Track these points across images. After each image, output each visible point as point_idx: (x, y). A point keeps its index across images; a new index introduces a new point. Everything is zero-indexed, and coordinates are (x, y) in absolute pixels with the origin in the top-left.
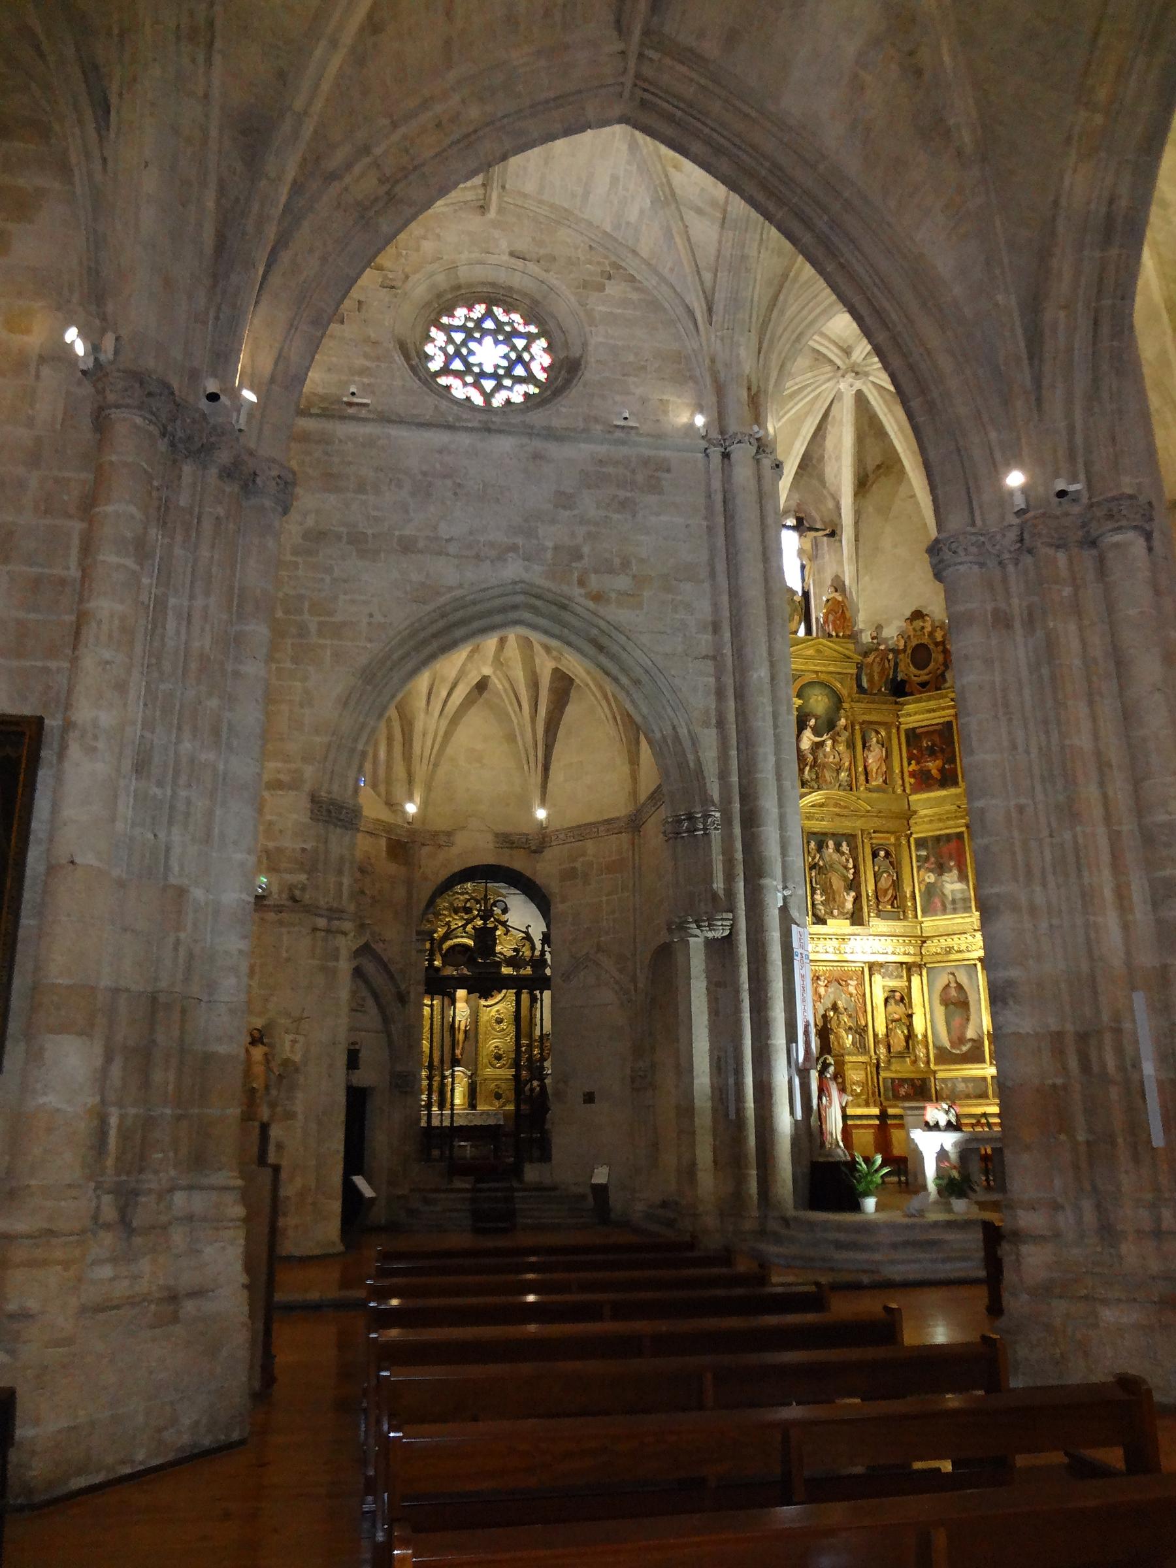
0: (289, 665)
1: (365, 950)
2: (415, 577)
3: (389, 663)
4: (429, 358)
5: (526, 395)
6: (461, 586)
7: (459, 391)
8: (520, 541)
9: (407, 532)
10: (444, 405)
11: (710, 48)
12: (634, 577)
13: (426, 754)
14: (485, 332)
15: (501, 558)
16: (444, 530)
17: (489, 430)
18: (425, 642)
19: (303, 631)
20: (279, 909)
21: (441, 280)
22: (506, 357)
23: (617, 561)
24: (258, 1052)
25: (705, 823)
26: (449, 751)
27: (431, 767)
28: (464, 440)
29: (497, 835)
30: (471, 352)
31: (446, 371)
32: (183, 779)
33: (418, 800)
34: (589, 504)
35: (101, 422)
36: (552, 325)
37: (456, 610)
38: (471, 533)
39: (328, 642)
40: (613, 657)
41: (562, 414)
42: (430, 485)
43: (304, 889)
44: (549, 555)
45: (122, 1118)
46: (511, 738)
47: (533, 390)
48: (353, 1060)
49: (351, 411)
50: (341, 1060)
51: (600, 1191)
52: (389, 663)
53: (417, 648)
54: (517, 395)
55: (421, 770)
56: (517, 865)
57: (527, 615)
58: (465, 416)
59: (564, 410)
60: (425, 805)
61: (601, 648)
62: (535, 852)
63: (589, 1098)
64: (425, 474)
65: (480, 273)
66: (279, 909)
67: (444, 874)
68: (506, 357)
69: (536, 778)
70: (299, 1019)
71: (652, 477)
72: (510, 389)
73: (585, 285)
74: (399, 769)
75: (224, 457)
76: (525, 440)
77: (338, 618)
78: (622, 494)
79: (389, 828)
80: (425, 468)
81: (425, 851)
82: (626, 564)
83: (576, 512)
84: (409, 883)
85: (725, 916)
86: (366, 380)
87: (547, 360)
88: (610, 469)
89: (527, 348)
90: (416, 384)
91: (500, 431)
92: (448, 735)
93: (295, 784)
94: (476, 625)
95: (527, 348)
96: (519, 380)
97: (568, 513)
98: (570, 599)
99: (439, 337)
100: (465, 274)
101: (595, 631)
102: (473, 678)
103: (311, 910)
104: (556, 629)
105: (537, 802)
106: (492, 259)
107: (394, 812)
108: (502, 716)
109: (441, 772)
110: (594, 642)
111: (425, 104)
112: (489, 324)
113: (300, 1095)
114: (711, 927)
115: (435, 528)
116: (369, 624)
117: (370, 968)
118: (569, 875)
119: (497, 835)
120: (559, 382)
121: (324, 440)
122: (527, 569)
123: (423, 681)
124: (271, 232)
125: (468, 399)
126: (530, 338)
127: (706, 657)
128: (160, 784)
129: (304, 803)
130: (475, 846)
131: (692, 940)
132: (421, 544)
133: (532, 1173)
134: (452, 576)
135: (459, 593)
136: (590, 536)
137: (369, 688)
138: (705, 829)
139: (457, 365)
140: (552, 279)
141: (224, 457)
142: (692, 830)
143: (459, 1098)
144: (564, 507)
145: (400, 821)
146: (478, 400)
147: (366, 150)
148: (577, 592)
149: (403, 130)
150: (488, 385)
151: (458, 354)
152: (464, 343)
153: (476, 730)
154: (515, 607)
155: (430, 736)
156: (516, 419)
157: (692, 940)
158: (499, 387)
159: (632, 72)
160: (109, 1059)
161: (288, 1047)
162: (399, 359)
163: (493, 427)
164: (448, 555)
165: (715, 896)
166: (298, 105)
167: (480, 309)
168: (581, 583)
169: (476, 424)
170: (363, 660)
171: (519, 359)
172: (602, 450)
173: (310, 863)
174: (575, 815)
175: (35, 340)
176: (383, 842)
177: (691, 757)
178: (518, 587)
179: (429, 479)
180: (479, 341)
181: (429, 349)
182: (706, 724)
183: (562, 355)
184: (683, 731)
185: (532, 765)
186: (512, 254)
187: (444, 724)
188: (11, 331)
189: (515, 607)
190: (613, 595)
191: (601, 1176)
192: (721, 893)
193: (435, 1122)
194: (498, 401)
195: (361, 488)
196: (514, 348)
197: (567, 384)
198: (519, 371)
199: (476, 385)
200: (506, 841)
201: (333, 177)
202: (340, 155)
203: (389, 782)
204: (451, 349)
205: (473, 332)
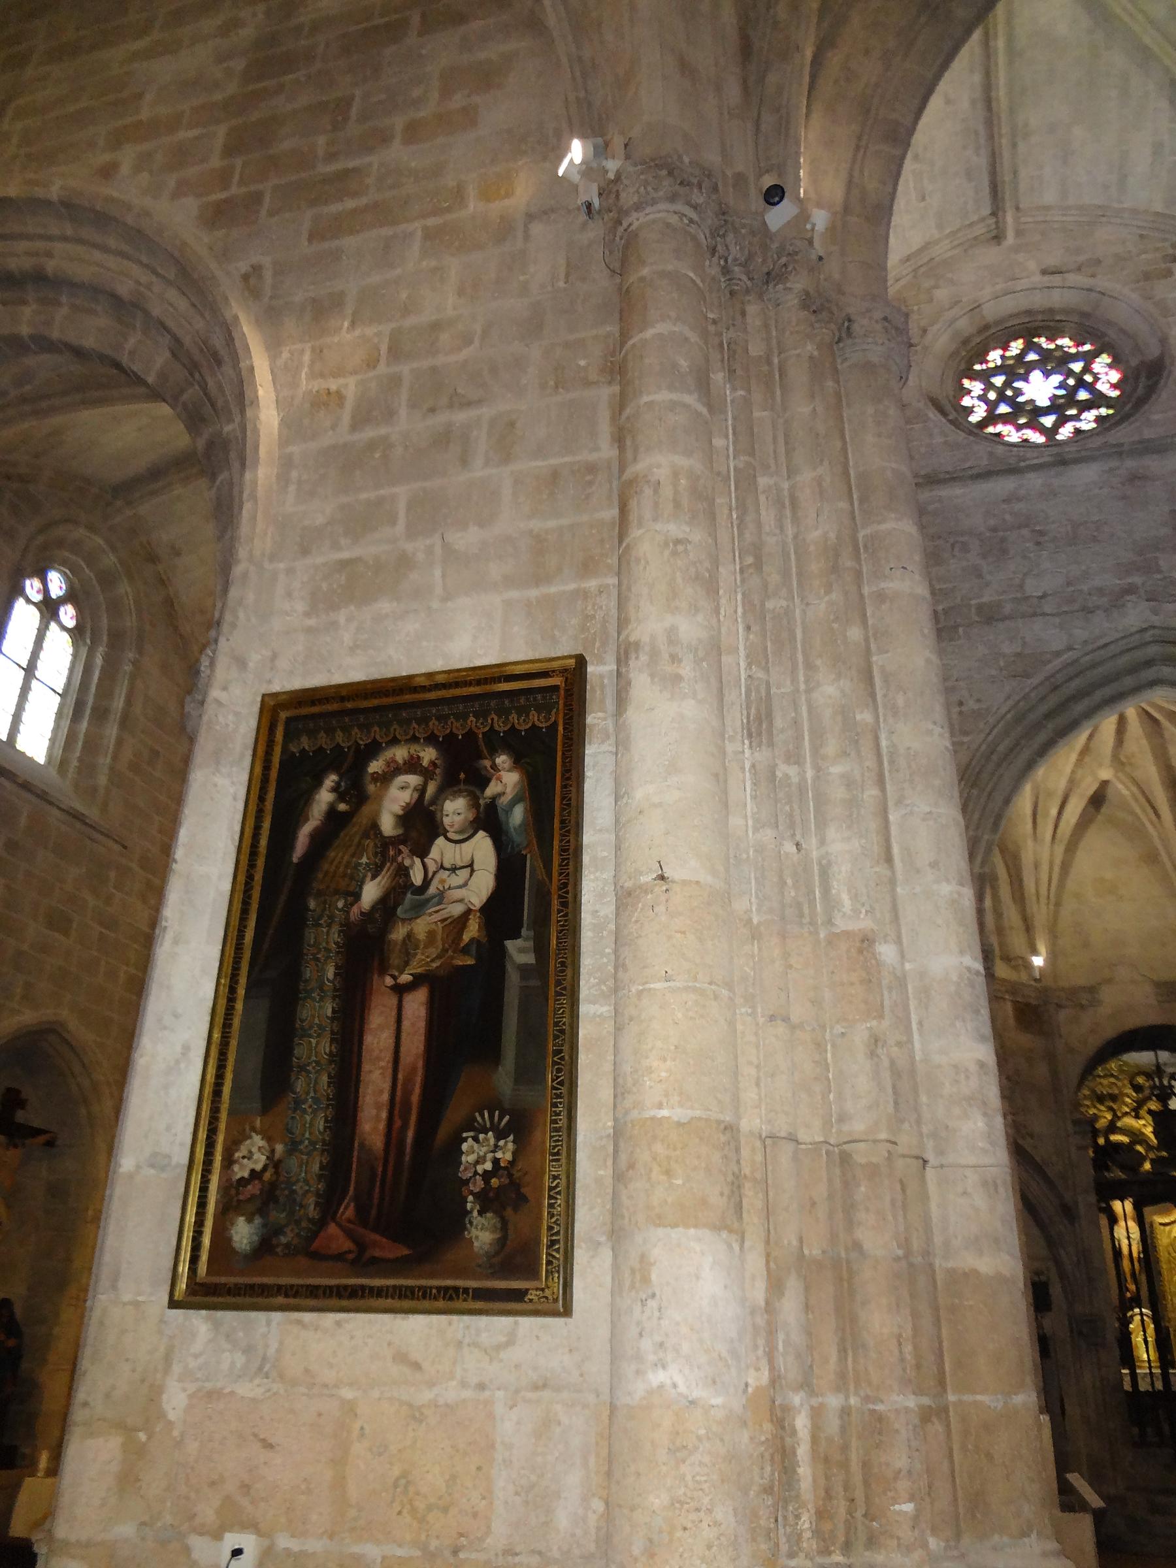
2: (1008, 649)
3: (995, 757)
4: (970, 411)
5: (1099, 419)
6: (1070, 648)
7: (1011, 435)
8: (1137, 579)
9: (985, 599)
10: (1000, 449)
13: (1043, 891)
14: (1031, 367)
16: (1033, 588)
18: (1038, 726)
21: (964, 325)
26: (1071, 885)
27: (1052, 907)
28: (1034, 481)
29: (1158, 985)
30: (1018, 392)
31: (992, 418)
32: (831, 747)
33: (1042, 948)
36: (1112, 334)
38: (1069, 584)
41: (1159, 417)
42: (1003, 540)
45: (817, 1414)
55: (1040, 913)
59: (1156, 417)
60: (1053, 957)
64: (994, 530)
65: (1010, 304)
67: (1095, 1043)
68: (1062, 385)
72: (1076, 418)
73: (1147, 276)
74: (1012, 915)
76: (1114, 463)
80: (992, 522)
81: (1063, 1015)
84: (1051, 1057)
87: (1115, 376)
89: (1087, 369)
91: (1076, 461)
92: (1066, 867)
94: (1098, 695)
95: (1087, 369)
96: (1086, 406)
99: (977, 387)
100: (991, 311)
102: (1089, 787)
106: (1024, 283)
107: (1015, 968)
108: (1134, 832)
112: (1032, 357)
115: (1021, 586)
116: (961, 713)
119: (1158, 985)
120: (1140, 391)
126: (1089, 358)
128: (793, 757)
132: (1008, 608)
135: (1067, 657)
137: (975, 792)
139: (1003, 409)
140: (1103, 282)
143: (1144, 1351)
145: (1024, 977)
146: (1037, 438)
150: (1048, 421)
151: (1002, 398)
152: (1008, 384)
153: (1100, 855)
154: (1149, 663)
155: (1045, 868)
160: (775, 1286)
162: (933, 414)
164: (1044, 614)
167: (1016, 347)
169: (1047, 459)
171: (1081, 383)
178: (1148, 636)
179: (1001, 534)
183: (1134, 362)
186: (1044, 272)
187: (1060, 850)
188: (488, 200)
189: (1149, 663)
193: (1144, 1386)
194: (1066, 432)
196: (1070, 373)
197: (1151, 390)
198: (1083, 395)
199: (1034, 425)
204: (992, 396)
205: (1016, 370)
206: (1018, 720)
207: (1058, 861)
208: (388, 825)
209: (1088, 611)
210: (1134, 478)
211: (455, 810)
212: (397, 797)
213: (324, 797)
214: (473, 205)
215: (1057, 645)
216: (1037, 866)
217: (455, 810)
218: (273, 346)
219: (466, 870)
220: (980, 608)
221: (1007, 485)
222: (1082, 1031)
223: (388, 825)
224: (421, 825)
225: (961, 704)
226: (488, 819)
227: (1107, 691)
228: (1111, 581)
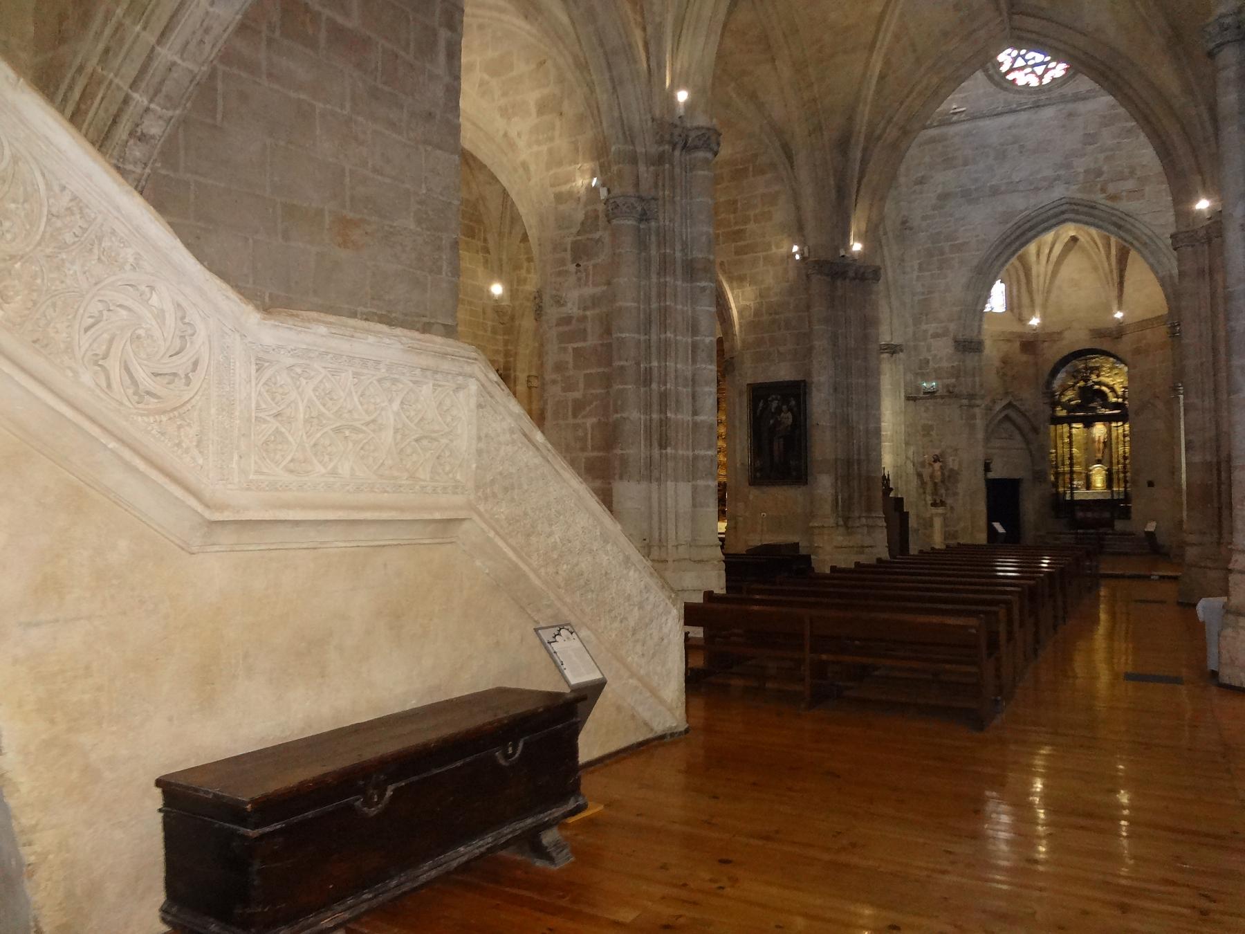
0: (937, 272)
1: (1010, 405)
4: (1001, 64)
8: (1062, 172)
10: (1010, 96)
15: (1050, 187)
18: (1010, 244)
20: (942, 397)
24: (937, 466)
26: (1057, 282)
28: (1023, 117)
35: (808, 276)
40: (1128, 231)
43: (954, 386)
44: (1081, 178)
46: (1095, 269)
48: (987, 468)
49: (955, 118)
50: (981, 469)
51: (1150, 535)
55: (1039, 299)
56: (1105, 348)
57: (1072, 216)
58: (1024, 101)
60: (1043, 317)
61: (1120, 227)
63: (1151, 484)
66: (942, 397)
69: (1115, 293)
70: (956, 450)
75: (851, 274)
76: (1062, 106)
79: (1020, 336)
81: (1046, 344)
82: (1132, 172)
84: (1036, 364)
90: (992, 89)
92: (1055, 273)
93: (945, 333)
103: (958, 396)
104: (1091, 220)
105: (1115, 307)
108: (1089, 257)
109: (1053, 296)
110: (1115, 224)
113: (959, 485)
117: (1013, 414)
118: (1137, 351)
121: (943, 139)
122: (1067, 189)
123: (1032, 248)
125: (1028, 84)
129: (950, 343)
130: (1078, 338)
133: (1119, 525)
134: (1021, 204)
136: (1107, 159)
141: (851, 274)
146: (1034, 82)
148: (1099, 198)
150: (1040, 70)
153: (1074, 267)
154: (1063, 213)
156: (1056, 93)
158: (1047, 70)
161: (952, 463)
168: (1103, 190)
170: (975, 262)
173: (957, 373)
174: (1140, 314)
175: (784, 250)
178: (1063, 201)
187: (1051, 267)
189: (1063, 213)
191: (1151, 527)
194: (1046, 80)
195: (965, 164)
200: (1099, 333)
201: (879, 138)
202: (882, 125)
203: (1020, 306)
206: (1002, 242)
207: (1049, 273)
209: (1037, 189)
210: (1070, 115)
212: (775, 404)
213: (761, 404)
214: (774, 250)
215: (1022, 208)
217: (784, 407)
218: (732, 289)
219: (787, 418)
220: (991, 187)
221: (1008, 120)
224: (779, 410)
226: (790, 410)
227: (1046, 225)
228: (1048, 173)
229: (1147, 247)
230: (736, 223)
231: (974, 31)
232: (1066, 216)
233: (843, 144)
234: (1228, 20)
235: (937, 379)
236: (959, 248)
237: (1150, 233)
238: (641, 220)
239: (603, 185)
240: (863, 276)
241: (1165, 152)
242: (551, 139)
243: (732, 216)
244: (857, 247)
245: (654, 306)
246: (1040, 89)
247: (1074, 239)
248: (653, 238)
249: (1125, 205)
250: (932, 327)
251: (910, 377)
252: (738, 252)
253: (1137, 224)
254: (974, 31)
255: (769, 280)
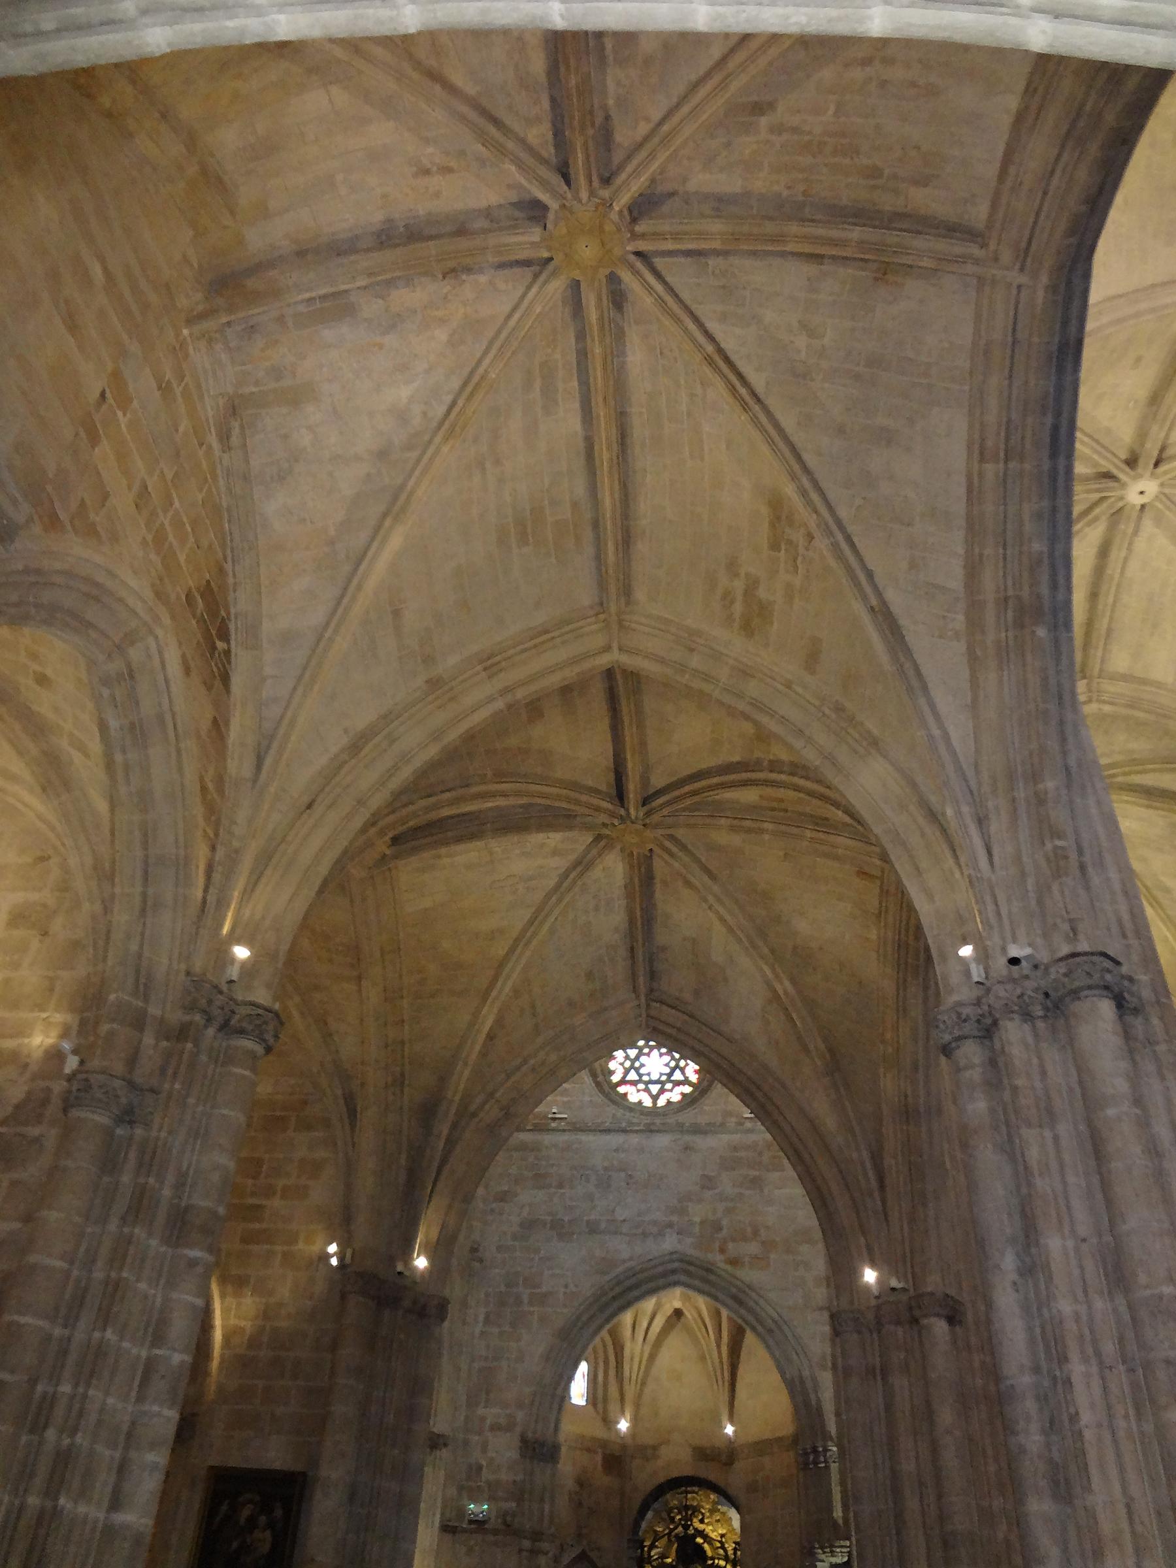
0: (507, 1328)
3: (580, 1324)
4: (612, 1073)
6: (631, 1259)
7: (634, 1095)
8: (675, 1218)
9: (592, 1217)
10: (620, 1113)
11: (687, 996)
12: (763, 1243)
13: (634, 1377)
15: (661, 1234)
16: (621, 1214)
17: (651, 1131)
19: (518, 1301)
20: (495, 1532)
22: (667, 1065)
23: (749, 1230)
25: (825, 1456)
26: (654, 1371)
28: (634, 1139)
34: (727, 1184)
35: (343, 1296)
37: (628, 1278)
38: (639, 1215)
39: (536, 1309)
40: (751, 1311)
44: (697, 1230)
46: (703, 1358)
47: (687, 1089)
49: (554, 1125)
52: (580, 1324)
53: (602, 1309)
54: (675, 1096)
55: (630, 1391)
57: (683, 1278)
58: (635, 1120)
60: (635, 1421)
61: (741, 1303)
62: (726, 1464)
64: (606, 1169)
66: (495, 1532)
68: (667, 1065)
69: (725, 1397)
71: (774, 1157)
74: (613, 1390)
75: (407, 1303)
77: (544, 1289)
78: (753, 1173)
79: (604, 1444)
80: (606, 1164)
82: (756, 1233)
83: (716, 1191)
85: (842, 1543)
86: (565, 1099)
88: (742, 1154)
90: (600, 1099)
91: (658, 1131)
92: (652, 1357)
93: (509, 1428)
96: (678, 1083)
97: (711, 1193)
98: (712, 1264)
101: (734, 1290)
102: (668, 1310)
104: (707, 1288)
105: (725, 1417)
108: (695, 1341)
109: (647, 1391)
110: (735, 1298)
111: (525, 1061)
114: (833, 1553)
115: (613, 1211)
116: (565, 1293)
118: (752, 1488)
120: (706, 1083)
121: (536, 1148)
122: (679, 1242)
123: (627, 1317)
124: (436, 1164)
125: (640, 1102)
127: (821, 1309)
129: (516, 1443)
130: (676, 1459)
131: (818, 1564)
132: (603, 1226)
134: (626, 1251)
135: (628, 1264)
136: (729, 1211)
138: (826, 1461)
139: (632, 1076)
142: (816, 1463)
144: (709, 1189)
146: (648, 1102)
147: (491, 1095)
148: (718, 1259)
149: (513, 1079)
150: (655, 1089)
153: (676, 1354)
155: (636, 1360)
156: (671, 1120)
157: (818, 1564)
158: (662, 1091)
159: (644, 1015)
163: (653, 1128)
165: (835, 1523)
166: (449, 1094)
168: (722, 1251)
169: (641, 1128)
172: (736, 1137)
173: (519, 1493)
174: (758, 1431)
175: (315, 1248)
176: (599, 1458)
177: (813, 1396)
180: (648, 1055)
181: (612, 1065)
182: (823, 1367)
184: (806, 1373)
185: (720, 1383)
187: (647, 1349)
189: (674, 1272)
190: (747, 1259)
192: (840, 1522)
194: (661, 1102)
195: (560, 1186)
198: (678, 1076)
199: (647, 1090)
200: (704, 1454)
201: (474, 1115)
202: (479, 1100)
203: (605, 1400)
207: (646, 1355)
208: (242, 1521)
209: (645, 1235)
211: (263, 1519)
212: (246, 1512)
213: (224, 1508)
214: (301, 1245)
216: (632, 1359)
218: (223, 1296)
219: (263, 1540)
220: (588, 1222)
221: (616, 1140)
222: (646, 1477)
223: (242, 1521)
224: (252, 1522)
225: (566, 1286)
229: (775, 1335)
230: (253, 1194)
231: (606, 1009)
232: (676, 1278)
233: (428, 1111)
234: (966, 1011)
235: (491, 1499)
236: (543, 1299)
237: (775, 1315)
238: (119, 1121)
239: (75, 1052)
240: (422, 1309)
241: (820, 1199)
242: (16, 966)
243: (250, 1182)
244: (421, 1263)
245: (99, 1275)
246: (654, 1111)
247: (678, 1313)
248: (132, 1155)
249: (748, 1275)
250: (492, 1413)
251: (452, 1491)
252: (245, 1240)
253: (762, 1302)
254: (606, 1009)
255: (284, 1292)
